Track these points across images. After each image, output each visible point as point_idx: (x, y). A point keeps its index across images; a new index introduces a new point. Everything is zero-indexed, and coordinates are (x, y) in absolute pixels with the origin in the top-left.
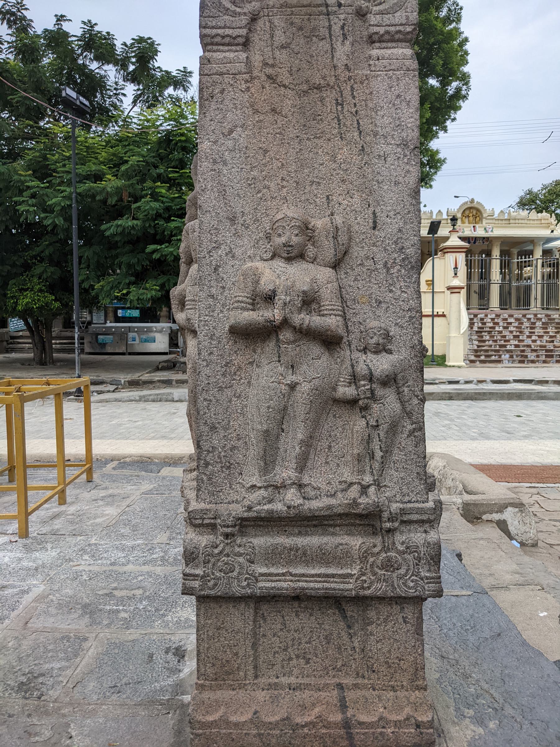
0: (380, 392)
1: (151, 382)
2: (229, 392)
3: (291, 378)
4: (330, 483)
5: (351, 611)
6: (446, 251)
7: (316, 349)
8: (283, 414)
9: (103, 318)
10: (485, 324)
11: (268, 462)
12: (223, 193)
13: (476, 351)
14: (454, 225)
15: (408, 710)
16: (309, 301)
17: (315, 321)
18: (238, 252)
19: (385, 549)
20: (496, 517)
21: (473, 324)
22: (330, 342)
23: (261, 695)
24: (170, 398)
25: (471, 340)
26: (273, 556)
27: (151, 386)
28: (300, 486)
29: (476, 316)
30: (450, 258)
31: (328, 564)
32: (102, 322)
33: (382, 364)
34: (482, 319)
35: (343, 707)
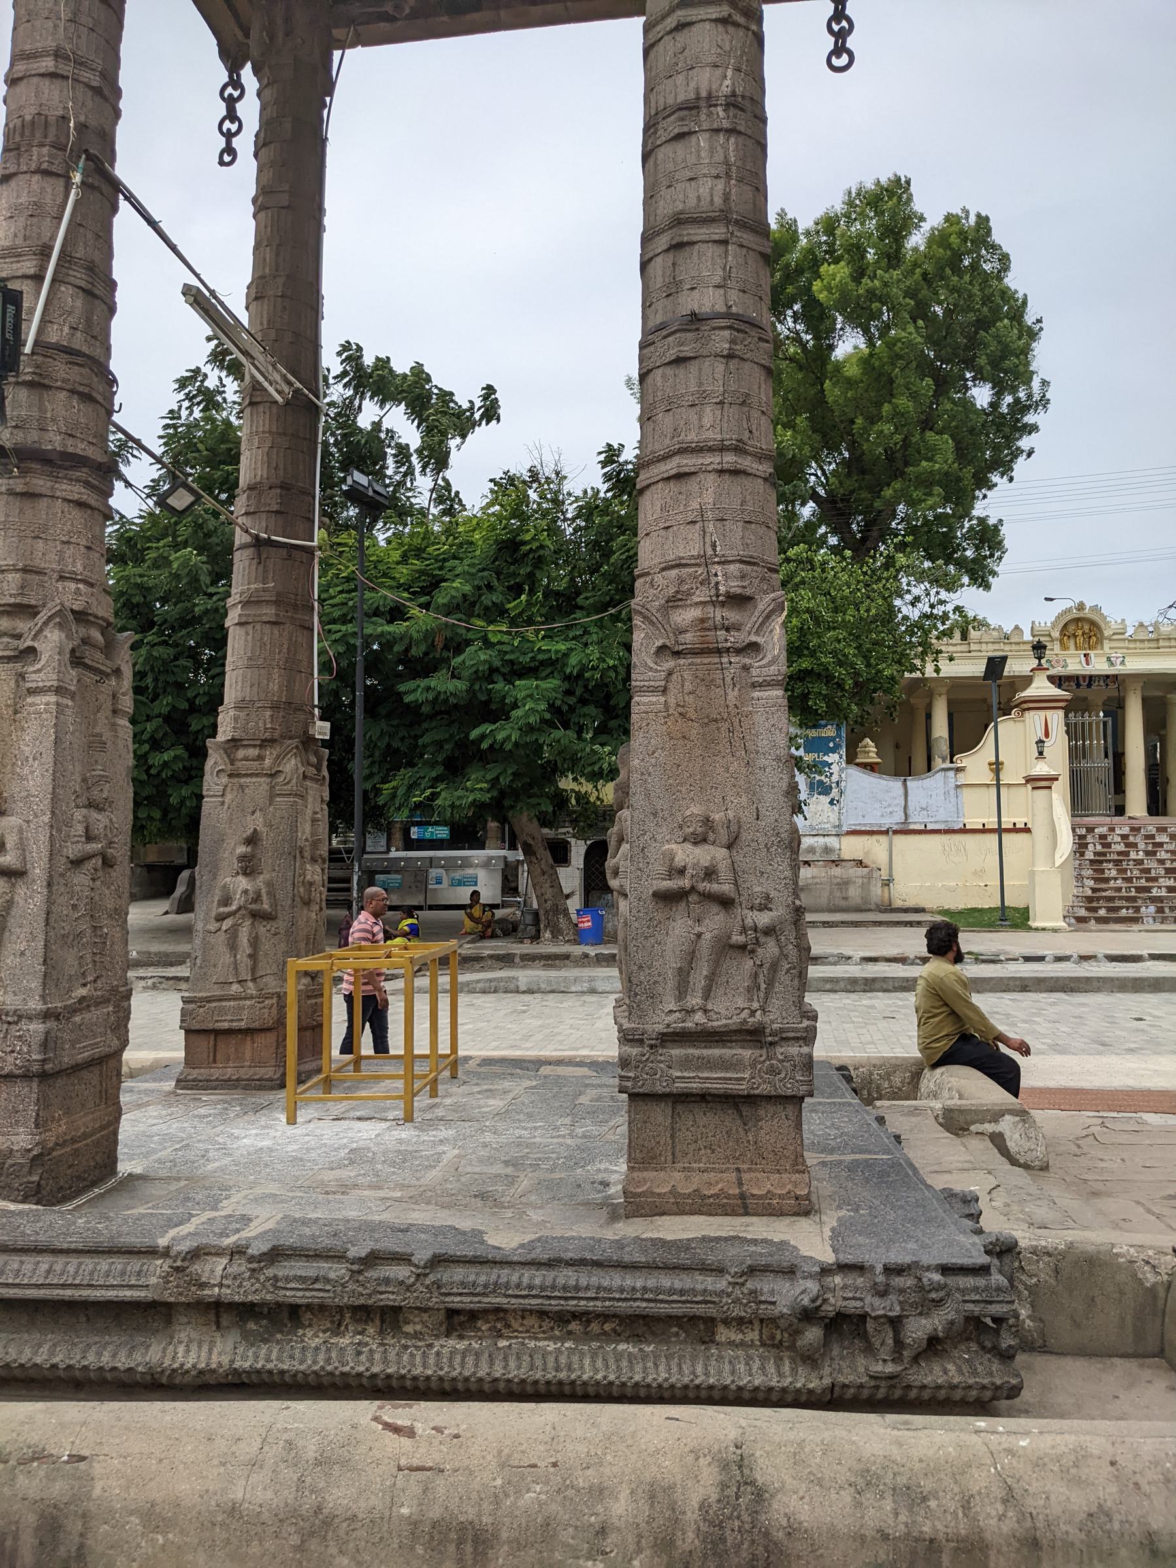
0: (762, 940)
1: (477, 959)
2: (652, 940)
3: (698, 929)
4: (728, 1009)
5: (746, 1111)
6: (1025, 706)
7: (715, 908)
8: (691, 957)
10: (1109, 845)
11: (682, 991)
12: (648, 795)
13: (1089, 899)
14: (1039, 658)
15: (789, 1187)
16: (710, 873)
17: (715, 887)
18: (659, 837)
19: (769, 1058)
20: (989, 1128)
21: (1086, 846)
22: (726, 903)
23: (677, 1175)
24: (512, 986)
25: (1079, 878)
26: (685, 1063)
27: (477, 966)
28: (706, 1011)
29: (1090, 830)
30: (1035, 720)
31: (727, 1070)
33: (764, 919)
34: (1103, 837)
35: (740, 1184)
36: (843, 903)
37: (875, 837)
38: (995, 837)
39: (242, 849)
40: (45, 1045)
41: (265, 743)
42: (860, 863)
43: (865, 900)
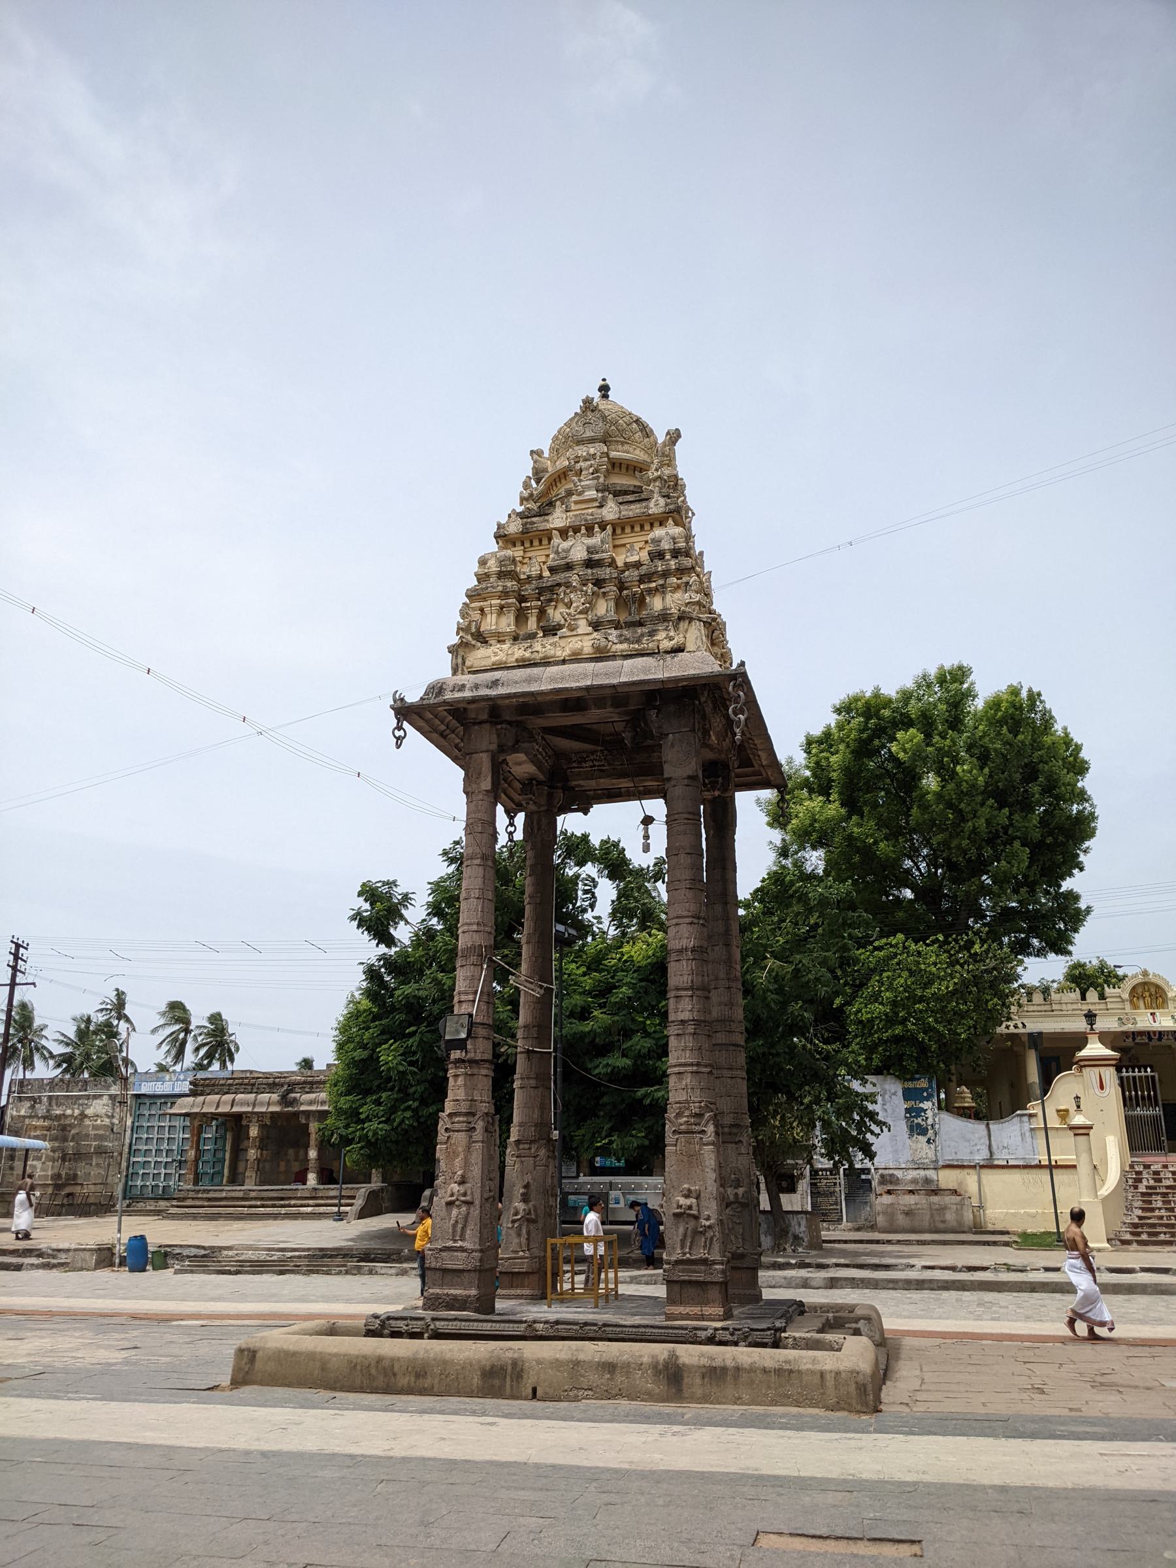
6: (1082, 1063)
8: (685, 1235)
9: (574, 1169)
10: (1160, 1180)
11: (682, 1247)
13: (1135, 1226)
14: (1092, 1024)
16: (690, 1207)
20: (854, 1325)
21: (1140, 1180)
22: (696, 1218)
25: (1129, 1208)
29: (1147, 1167)
30: (1091, 1074)
32: (574, 1175)
33: (708, 1223)
34: (1156, 1173)
36: (941, 1226)
37: (966, 1171)
38: (1045, 1176)
39: (522, 1191)
40: (481, 1260)
41: (532, 1142)
42: (955, 1192)
43: (960, 1223)
